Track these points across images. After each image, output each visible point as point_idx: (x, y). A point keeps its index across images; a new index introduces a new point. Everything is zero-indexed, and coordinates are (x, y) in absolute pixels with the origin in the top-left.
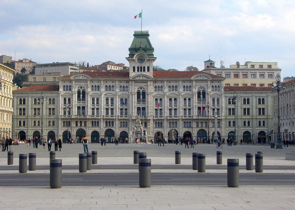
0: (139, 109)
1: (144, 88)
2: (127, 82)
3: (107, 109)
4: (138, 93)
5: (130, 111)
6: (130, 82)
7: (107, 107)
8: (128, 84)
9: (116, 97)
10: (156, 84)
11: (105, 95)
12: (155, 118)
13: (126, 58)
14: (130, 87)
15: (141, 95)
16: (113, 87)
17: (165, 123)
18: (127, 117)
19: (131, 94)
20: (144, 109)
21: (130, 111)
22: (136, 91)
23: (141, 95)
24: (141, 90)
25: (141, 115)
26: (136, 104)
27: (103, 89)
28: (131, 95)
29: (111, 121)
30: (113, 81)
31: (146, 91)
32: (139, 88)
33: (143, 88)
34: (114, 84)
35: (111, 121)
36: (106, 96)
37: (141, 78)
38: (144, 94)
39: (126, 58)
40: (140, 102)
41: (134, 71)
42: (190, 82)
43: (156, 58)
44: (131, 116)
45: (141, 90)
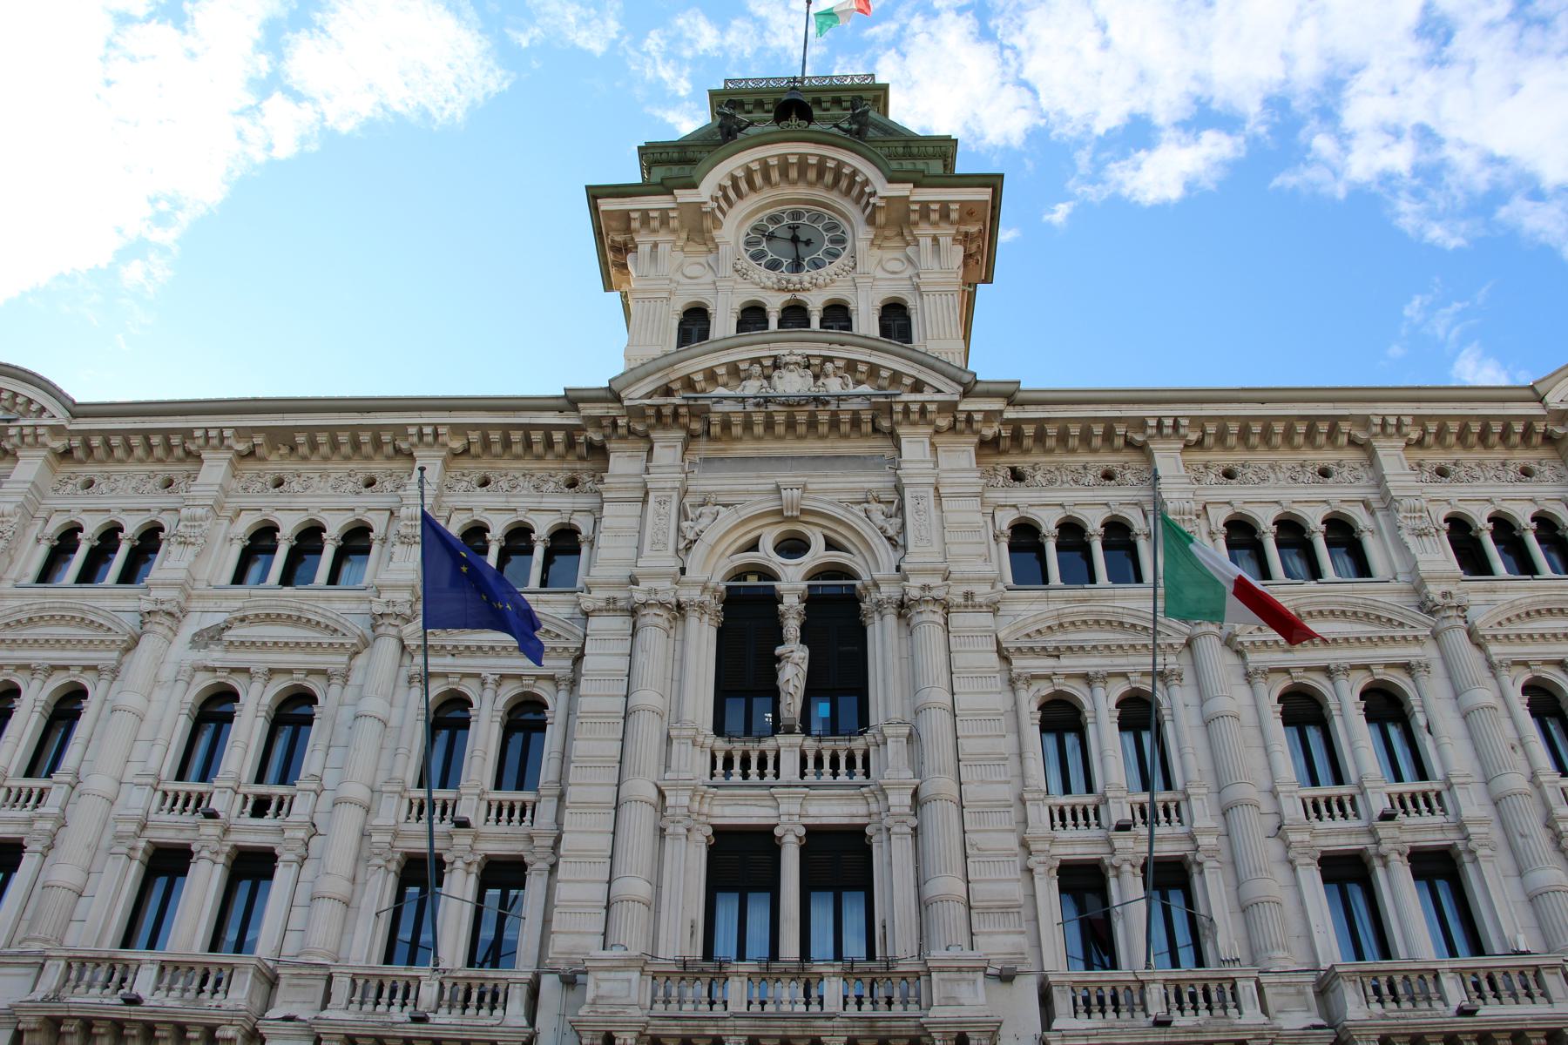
0: (739, 861)
1: (831, 545)
2: (572, 484)
3: (167, 864)
4: (746, 616)
5: (578, 887)
6: (623, 463)
7: (172, 829)
8: (583, 501)
11: (211, 637)
12: (1083, 1023)
13: (595, 194)
15: (792, 627)
18: (494, 998)
19: (611, 606)
20: (840, 860)
21: (563, 892)
22: (719, 582)
23: (792, 627)
24: (792, 579)
25: (790, 947)
26: (693, 764)
27: (197, 563)
28: (621, 623)
30: (377, 467)
31: (874, 568)
32: (753, 546)
33: (818, 544)
36: (215, 656)
38: (838, 617)
39: (595, 194)
40: (769, 744)
42: (1526, 472)
43: (994, 182)
44: (570, 981)
45: (792, 579)
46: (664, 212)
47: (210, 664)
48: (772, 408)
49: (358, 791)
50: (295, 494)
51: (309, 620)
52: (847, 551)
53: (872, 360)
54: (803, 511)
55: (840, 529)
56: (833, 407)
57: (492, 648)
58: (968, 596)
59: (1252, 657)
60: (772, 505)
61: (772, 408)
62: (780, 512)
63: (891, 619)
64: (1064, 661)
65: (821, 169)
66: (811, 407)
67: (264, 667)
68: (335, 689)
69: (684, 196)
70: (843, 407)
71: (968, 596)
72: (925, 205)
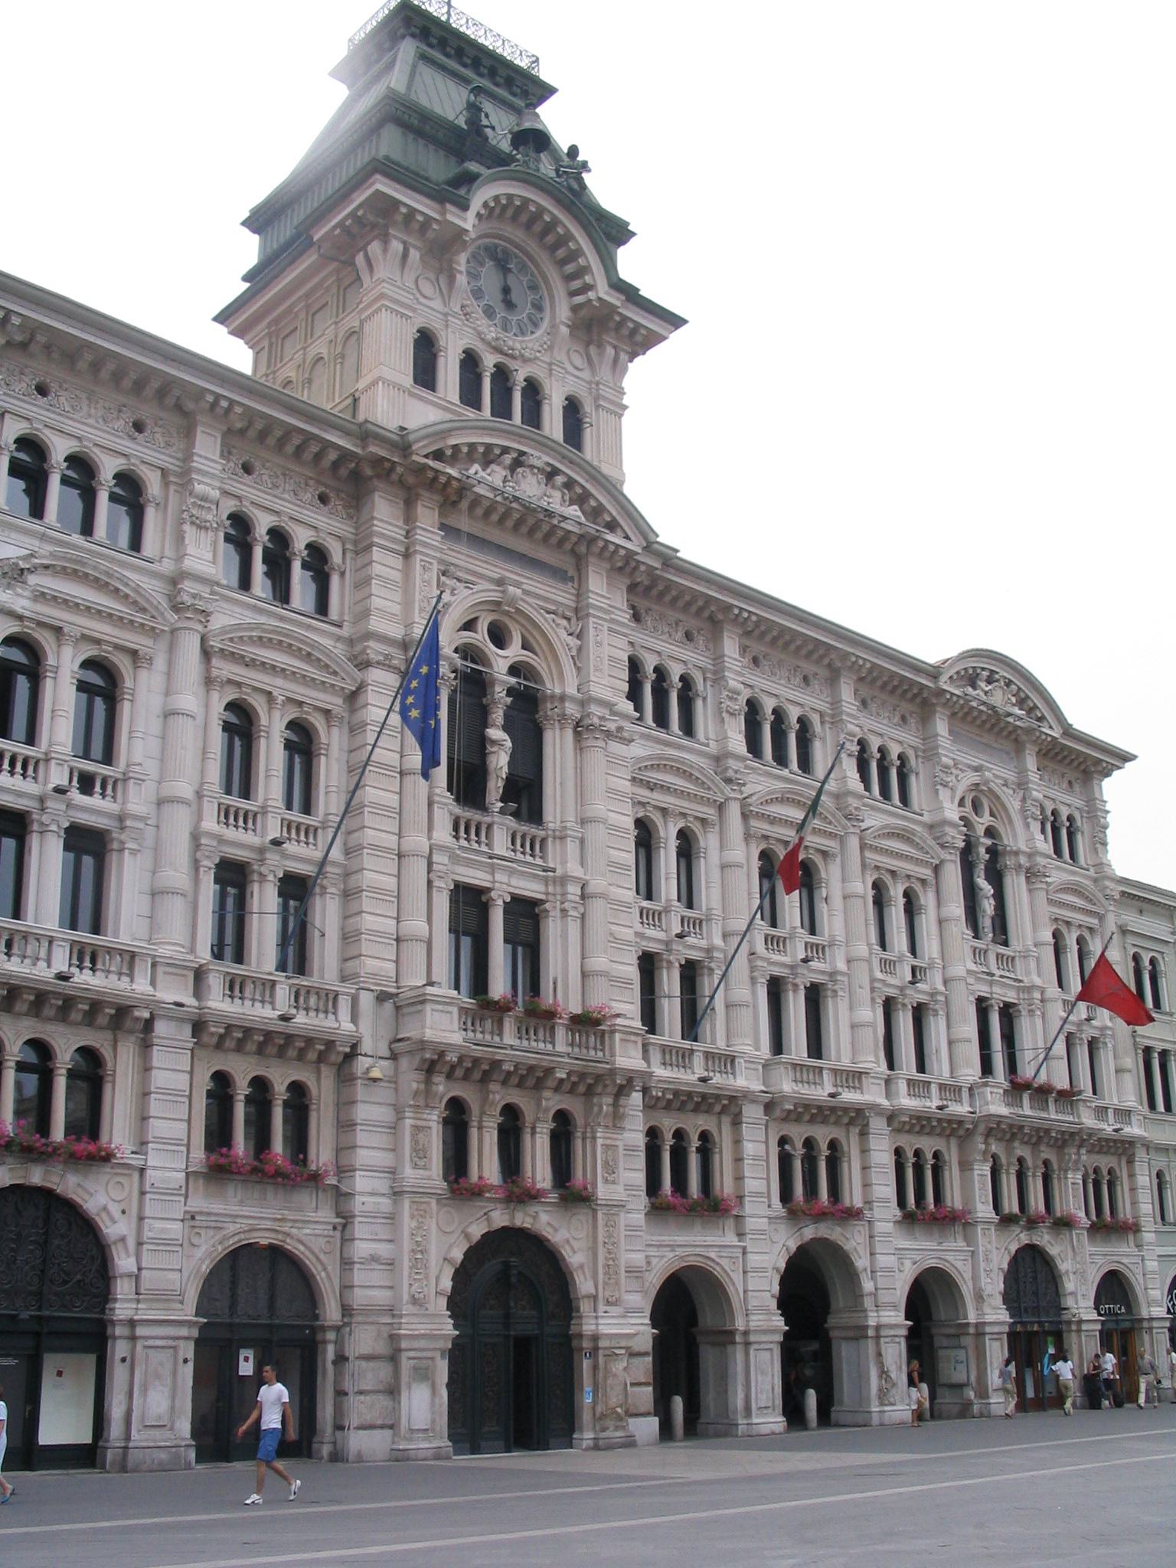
5: (376, 919)
9: (160, 663)
10: (640, 637)
14: (384, 564)
15: (498, 716)
16: (130, 492)
17: (750, 1148)
23: (498, 716)
29: (65, 1046)
30: (147, 412)
32: (469, 625)
34: (148, 457)
35: (65, 1046)
36: (21, 603)
37: (530, 488)
41: (425, 374)
46: (429, 219)
47: (20, 611)
48: (514, 505)
49: (186, 790)
50: (64, 413)
51: (117, 590)
52: (535, 654)
53: (588, 486)
54: (519, 611)
55: (535, 633)
56: (555, 522)
57: (284, 670)
58: (620, 729)
59: (753, 823)
60: (495, 596)
61: (514, 505)
62: (498, 604)
63: (569, 733)
64: (655, 795)
65: (549, 228)
66: (541, 516)
67: (77, 632)
68: (143, 674)
69: (453, 216)
70: (563, 525)
71: (620, 729)
72: (625, 319)
